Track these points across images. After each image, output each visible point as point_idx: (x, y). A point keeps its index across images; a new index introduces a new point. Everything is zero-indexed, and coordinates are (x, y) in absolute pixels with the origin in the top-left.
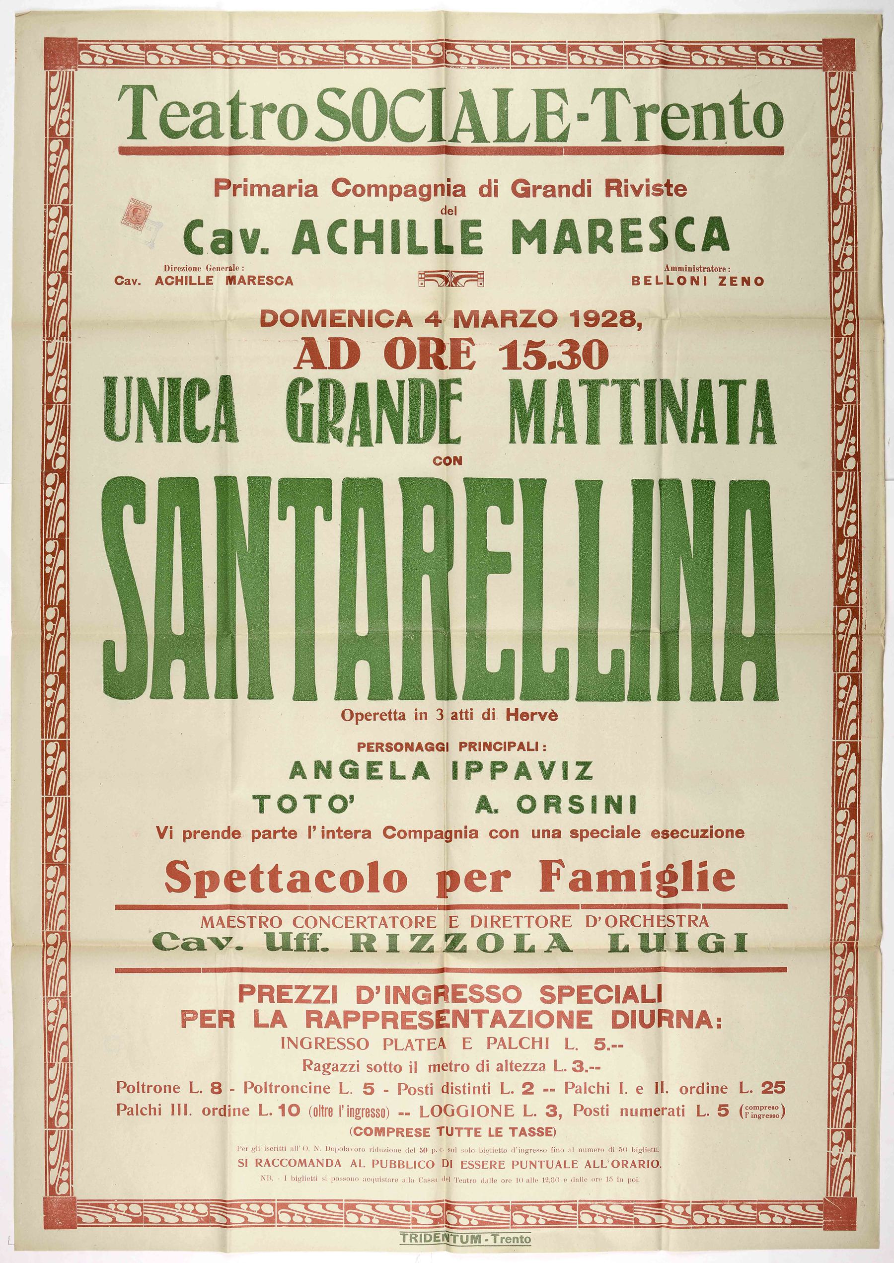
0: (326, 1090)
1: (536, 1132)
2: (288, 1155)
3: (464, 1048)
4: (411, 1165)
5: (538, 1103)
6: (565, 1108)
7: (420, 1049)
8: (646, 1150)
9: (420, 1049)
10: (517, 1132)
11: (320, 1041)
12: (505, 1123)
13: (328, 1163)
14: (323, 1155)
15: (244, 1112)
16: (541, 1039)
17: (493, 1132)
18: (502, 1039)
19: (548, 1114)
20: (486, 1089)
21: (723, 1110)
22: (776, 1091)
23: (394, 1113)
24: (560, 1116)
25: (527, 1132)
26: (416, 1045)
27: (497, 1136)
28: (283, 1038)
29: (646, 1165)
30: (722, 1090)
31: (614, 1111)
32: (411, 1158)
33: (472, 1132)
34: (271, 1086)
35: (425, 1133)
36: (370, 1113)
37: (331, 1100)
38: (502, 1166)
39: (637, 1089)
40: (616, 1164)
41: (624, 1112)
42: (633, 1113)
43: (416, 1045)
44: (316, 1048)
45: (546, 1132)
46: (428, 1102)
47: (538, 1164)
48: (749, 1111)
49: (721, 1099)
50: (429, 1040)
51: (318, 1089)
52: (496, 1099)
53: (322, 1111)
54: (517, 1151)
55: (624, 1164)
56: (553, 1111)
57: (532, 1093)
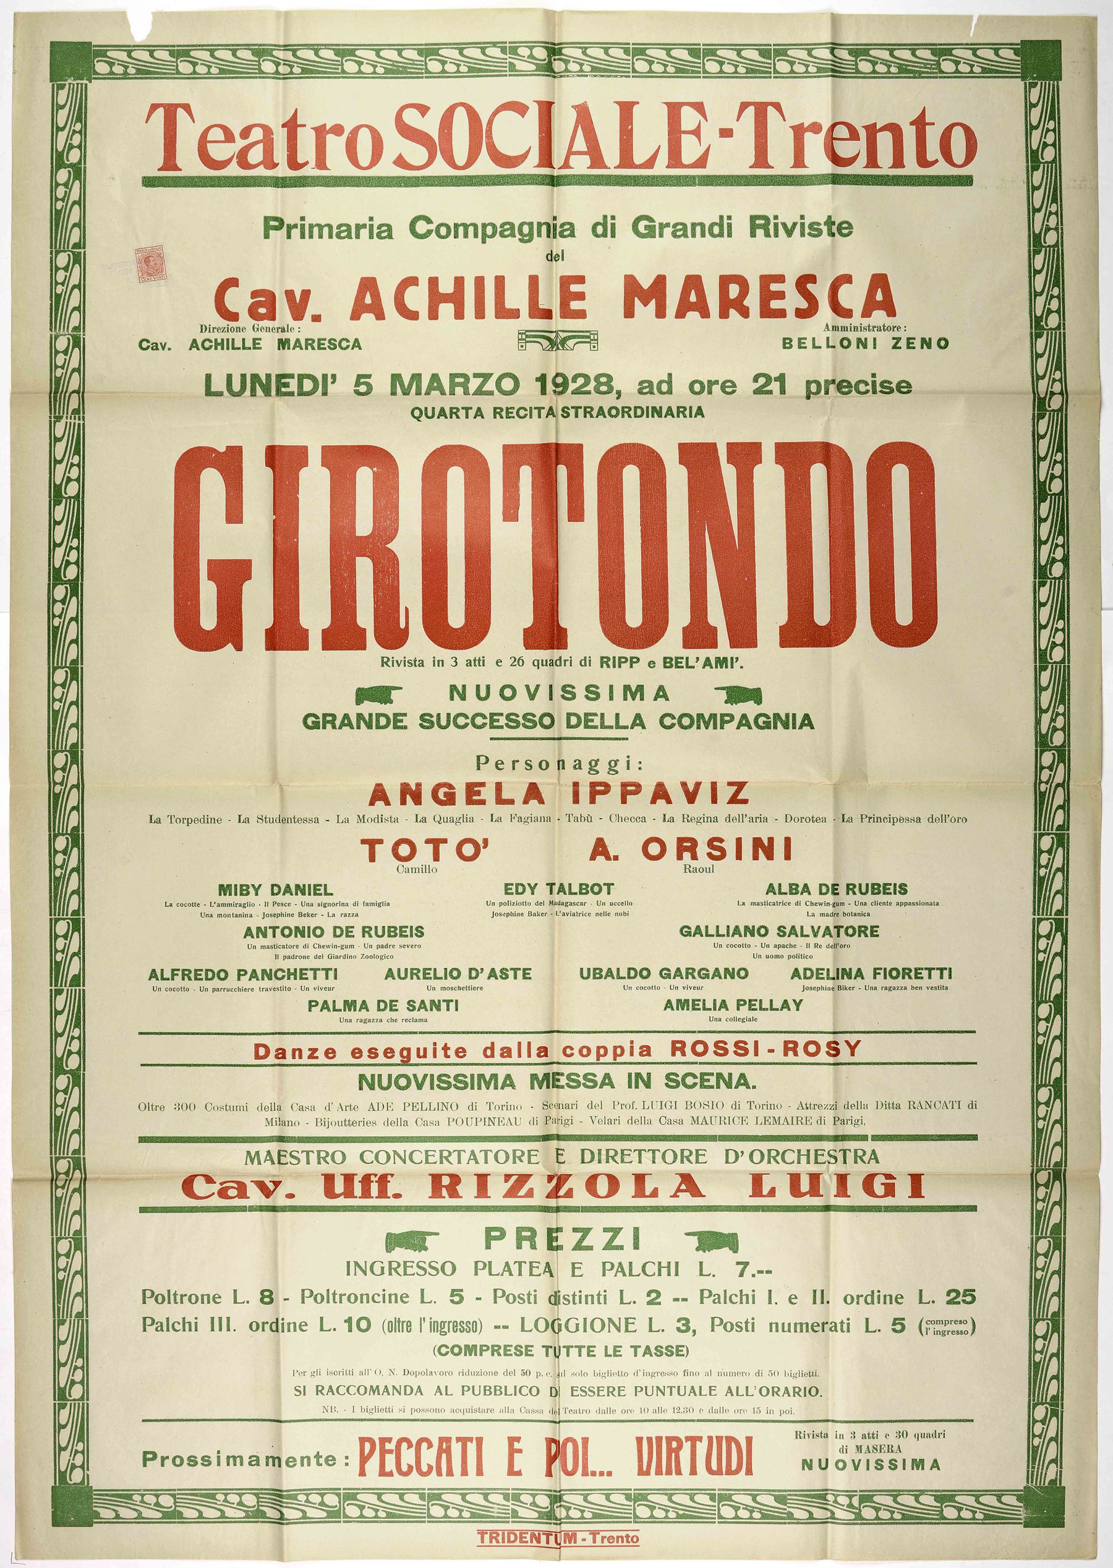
0: (403, 1298)
1: (664, 1350)
2: (356, 1380)
3: (573, 1275)
4: (511, 1391)
5: (667, 1314)
6: (699, 1322)
7: (520, 1274)
8: (802, 1374)
9: (520, 1274)
10: (641, 1351)
11: (394, 1265)
12: (625, 1340)
13: (408, 1391)
14: (400, 1381)
15: (302, 1327)
17: (610, 1351)
18: (620, 1264)
19: (678, 1329)
20: (602, 1298)
21: (899, 1325)
22: (964, 1301)
23: (488, 1326)
24: (694, 1331)
25: (653, 1351)
26: (515, 1269)
27: (615, 1355)
28: (348, 1263)
29: (802, 1393)
30: (898, 1299)
31: (762, 1326)
32: (510, 1382)
33: (584, 1351)
34: (334, 1294)
35: (525, 1351)
36: (458, 1326)
37: (410, 1312)
38: (622, 1393)
39: (790, 1298)
40: (764, 1392)
41: (773, 1327)
42: (785, 1328)
43: (515, 1269)
44: (390, 1274)
45: (677, 1351)
46: (532, 1313)
47: (667, 1391)
48: (930, 1326)
49: (895, 1311)
50: (531, 1263)
51: (393, 1297)
52: (612, 1310)
53: (396, 1326)
54: (641, 1374)
55: (775, 1391)
56: (685, 1325)
57: (659, 1303)
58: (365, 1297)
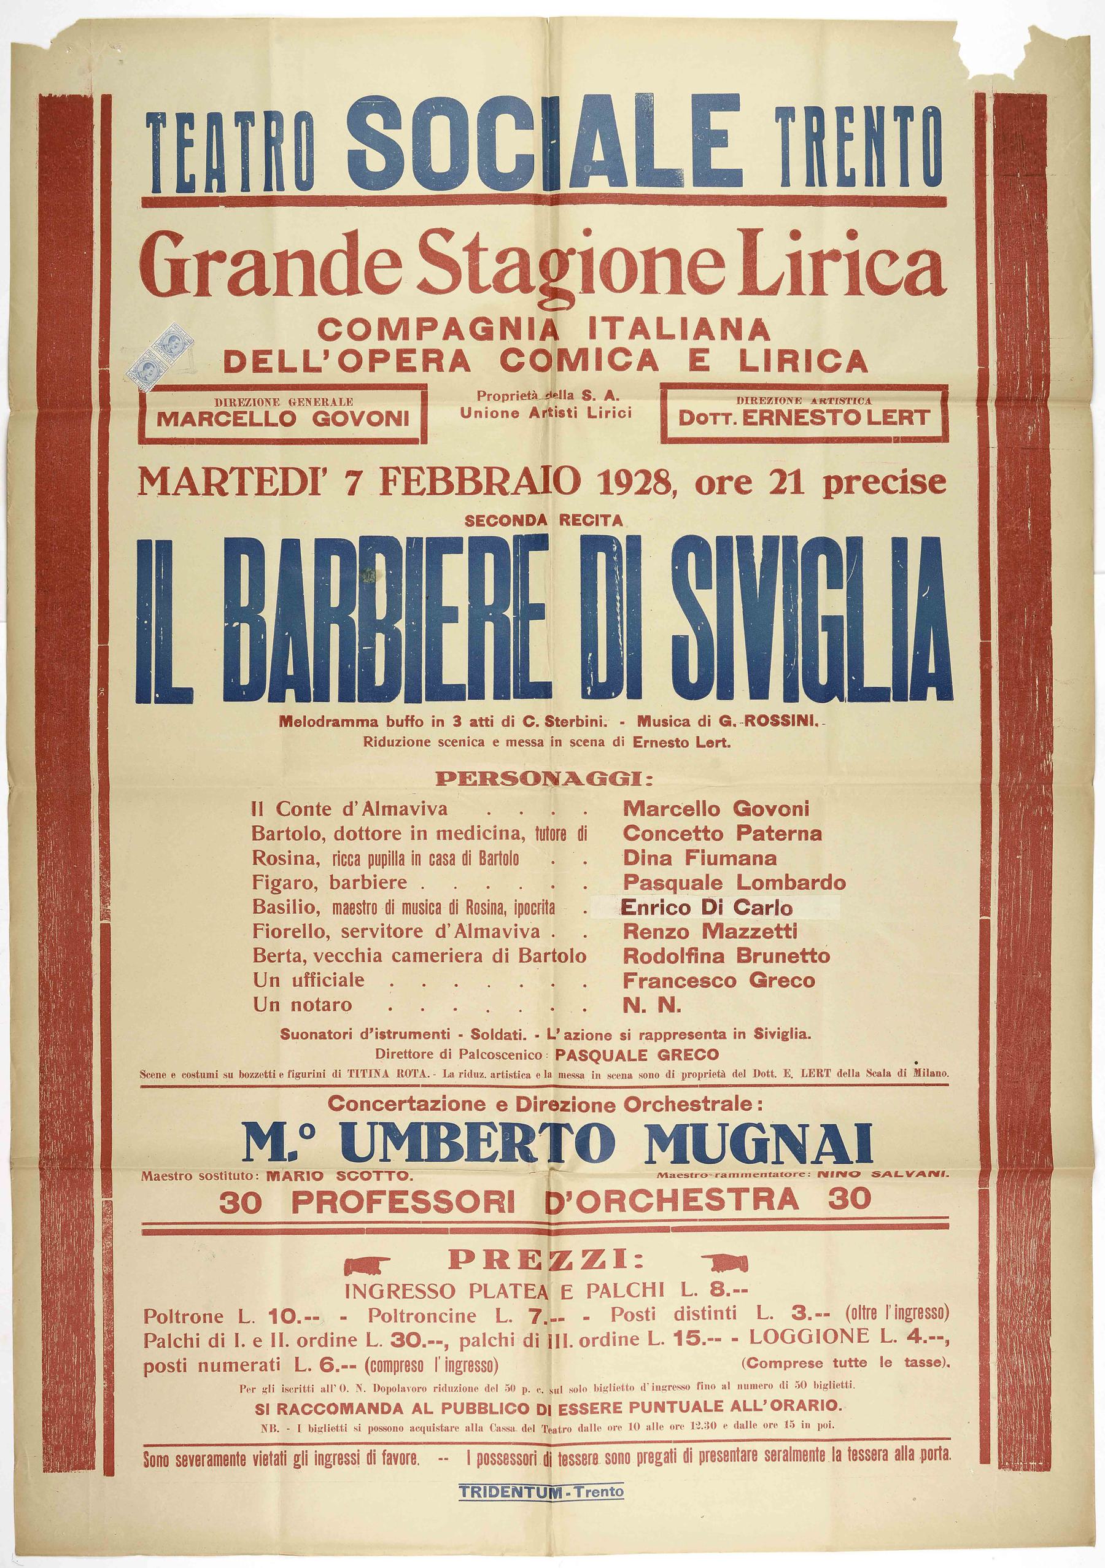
3: (563, 1298)
7: (516, 1296)
9: (516, 1296)
11: (393, 1288)
16: (654, 1284)
18: (605, 1286)
26: (510, 1291)
28: (348, 1286)
43: (510, 1291)
44: (389, 1297)
50: (526, 1285)
58: (432, 1317)
